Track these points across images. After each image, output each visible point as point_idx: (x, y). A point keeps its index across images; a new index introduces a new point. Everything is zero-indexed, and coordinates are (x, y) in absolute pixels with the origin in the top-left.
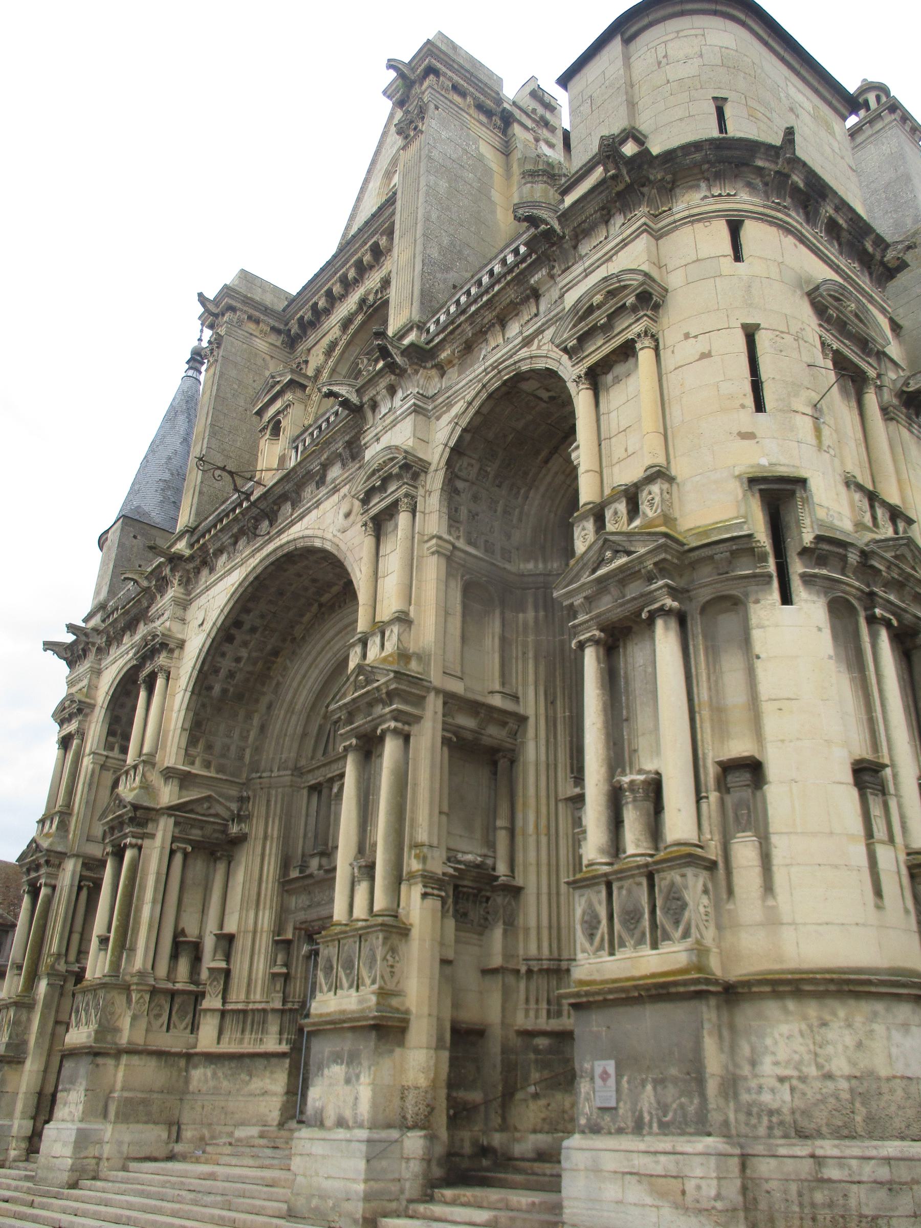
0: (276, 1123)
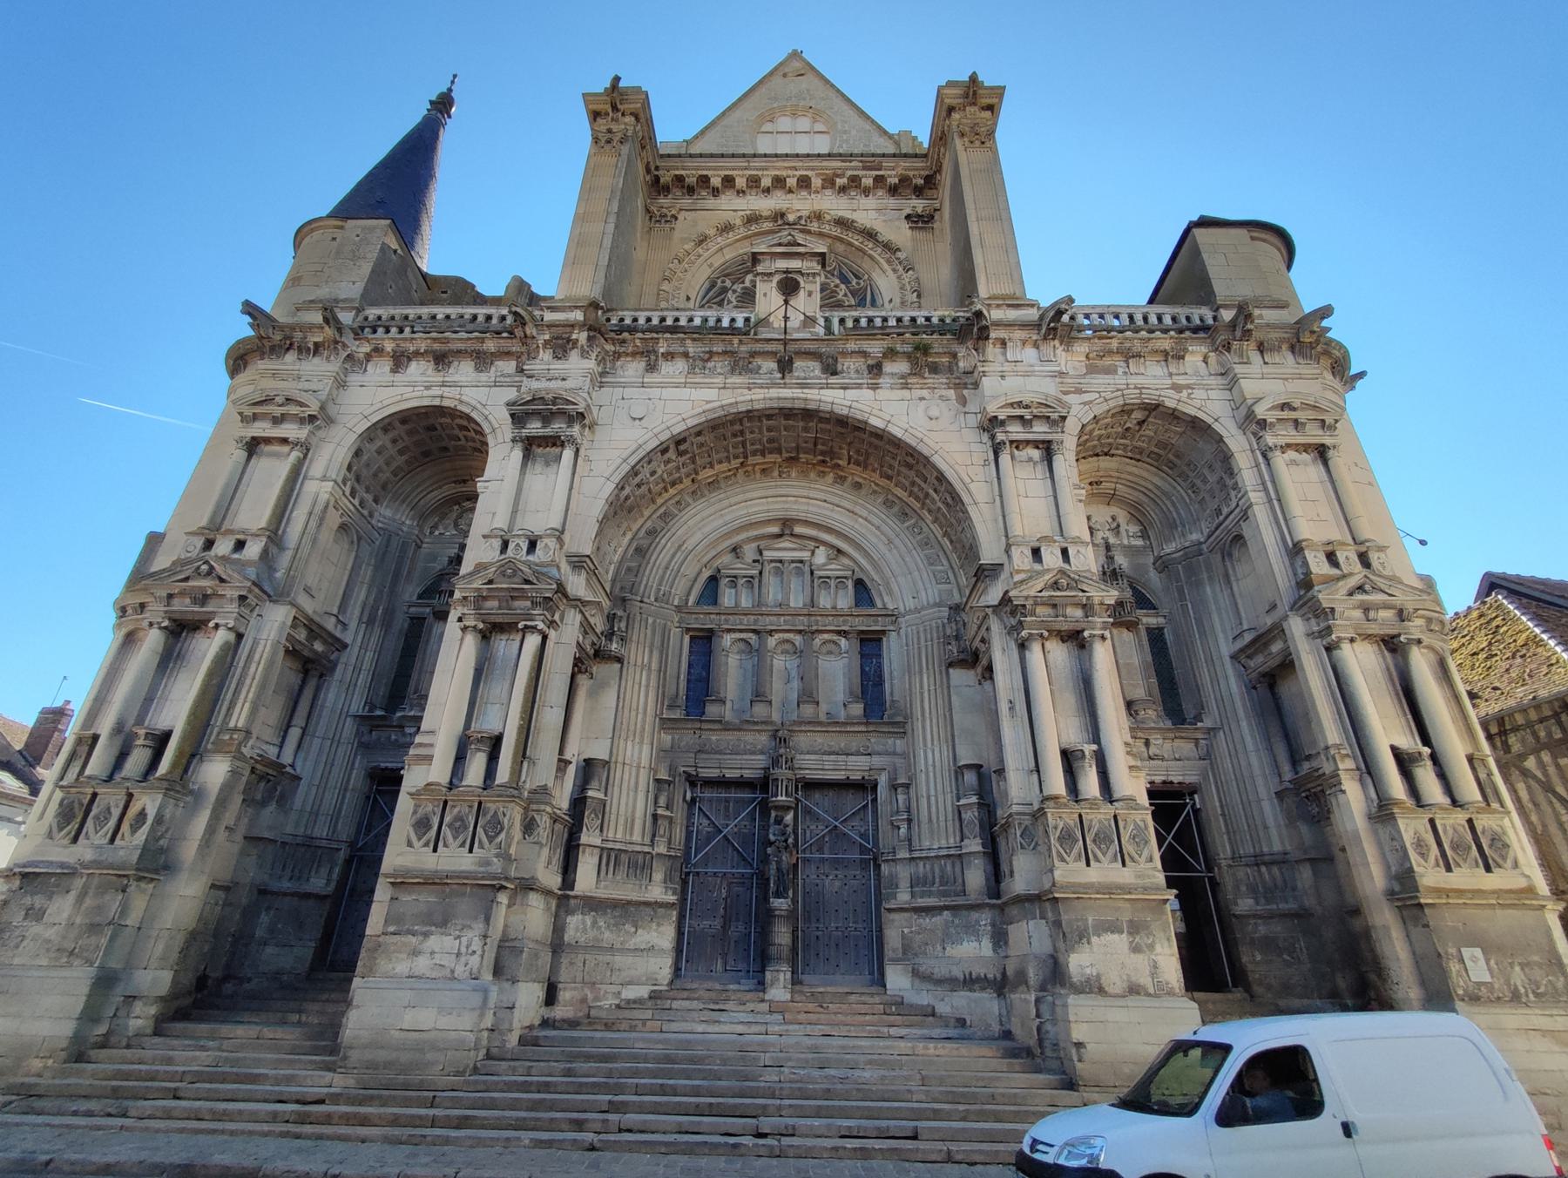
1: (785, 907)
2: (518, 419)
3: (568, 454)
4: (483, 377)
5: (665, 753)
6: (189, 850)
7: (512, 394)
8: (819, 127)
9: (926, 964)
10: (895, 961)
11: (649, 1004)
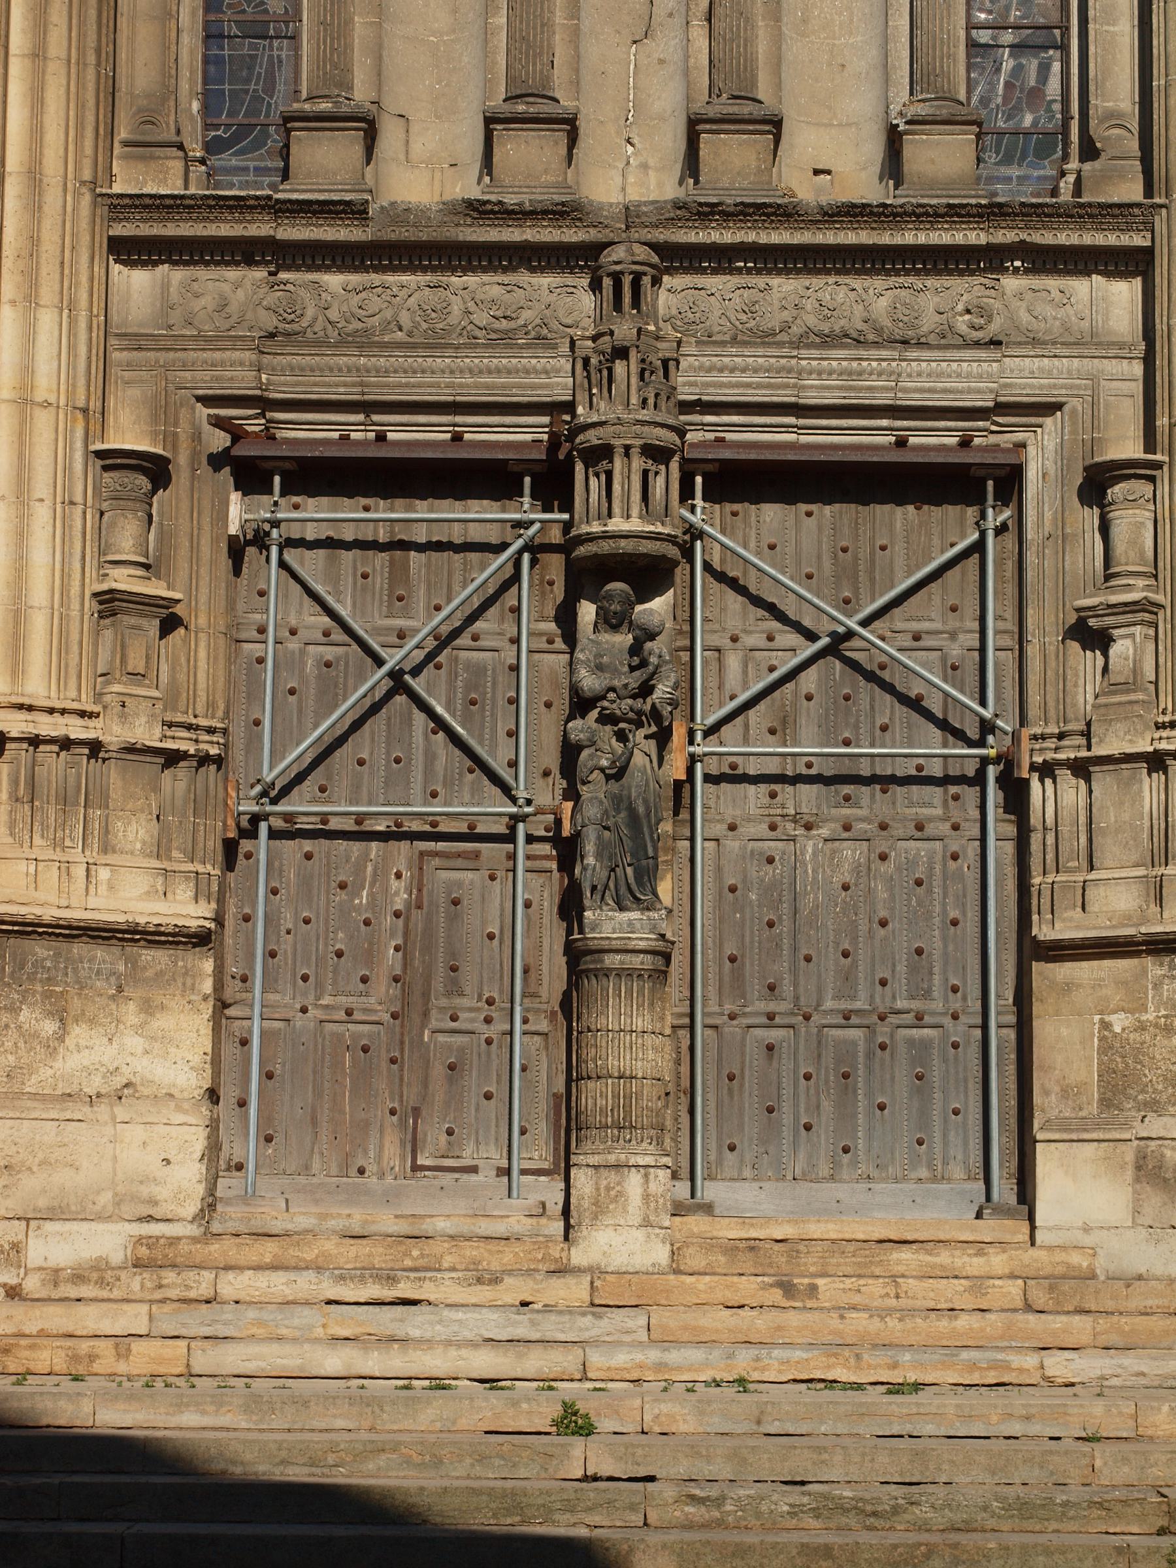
0: (191, 1208)
1: (643, 938)
5: (112, 345)
10: (1074, 1132)
11: (135, 1283)
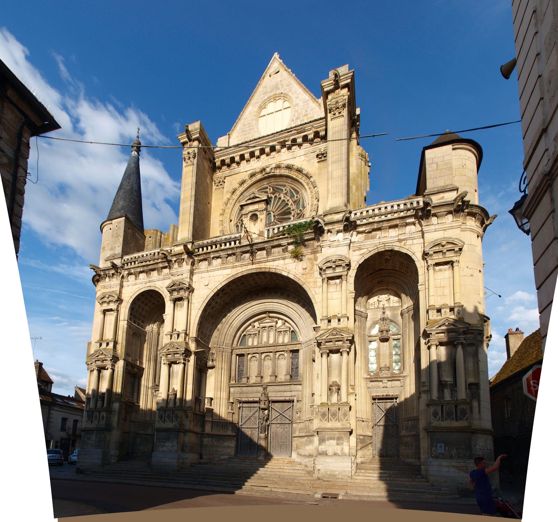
2: (171, 292)
3: (185, 303)
4: (160, 277)
6: (115, 424)
7: (168, 282)
8: (287, 104)
9: (302, 452)
